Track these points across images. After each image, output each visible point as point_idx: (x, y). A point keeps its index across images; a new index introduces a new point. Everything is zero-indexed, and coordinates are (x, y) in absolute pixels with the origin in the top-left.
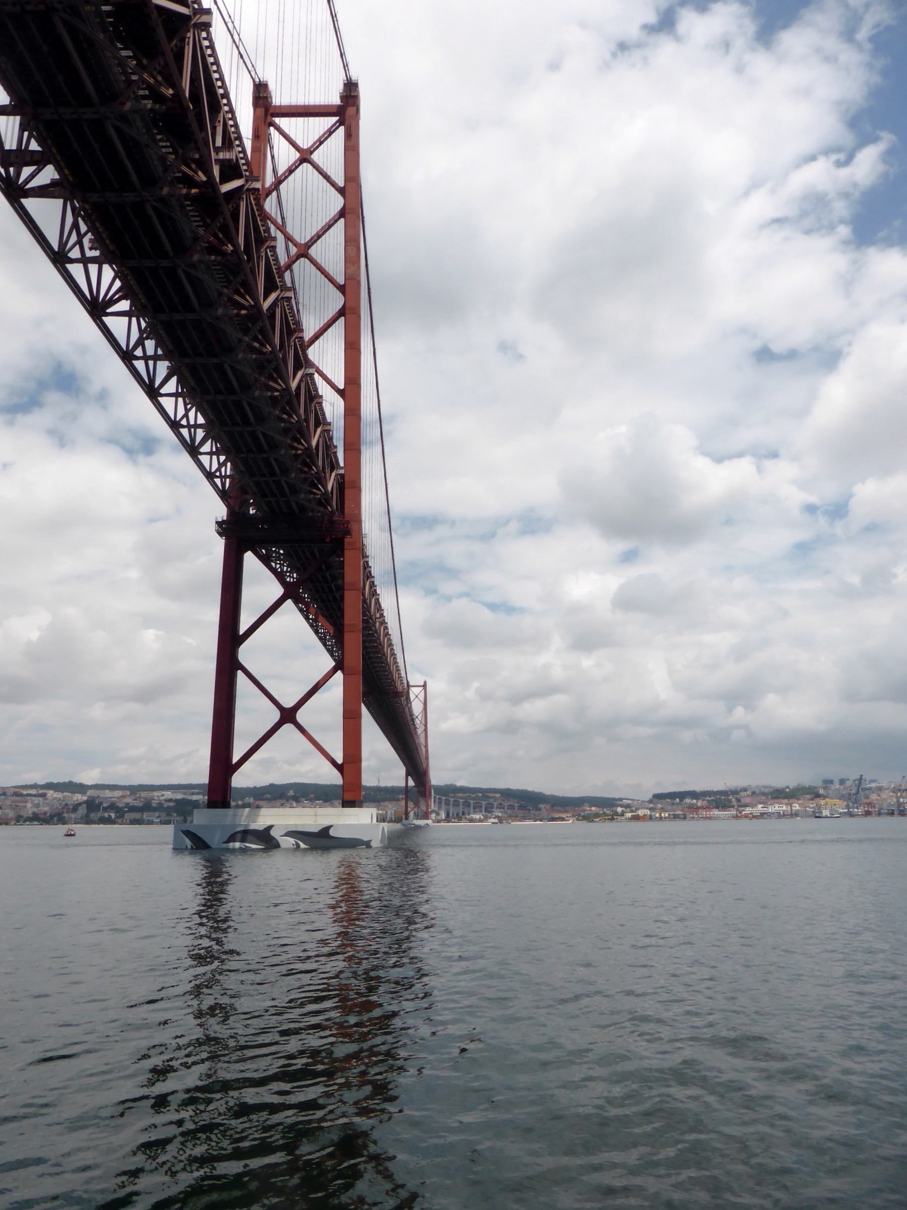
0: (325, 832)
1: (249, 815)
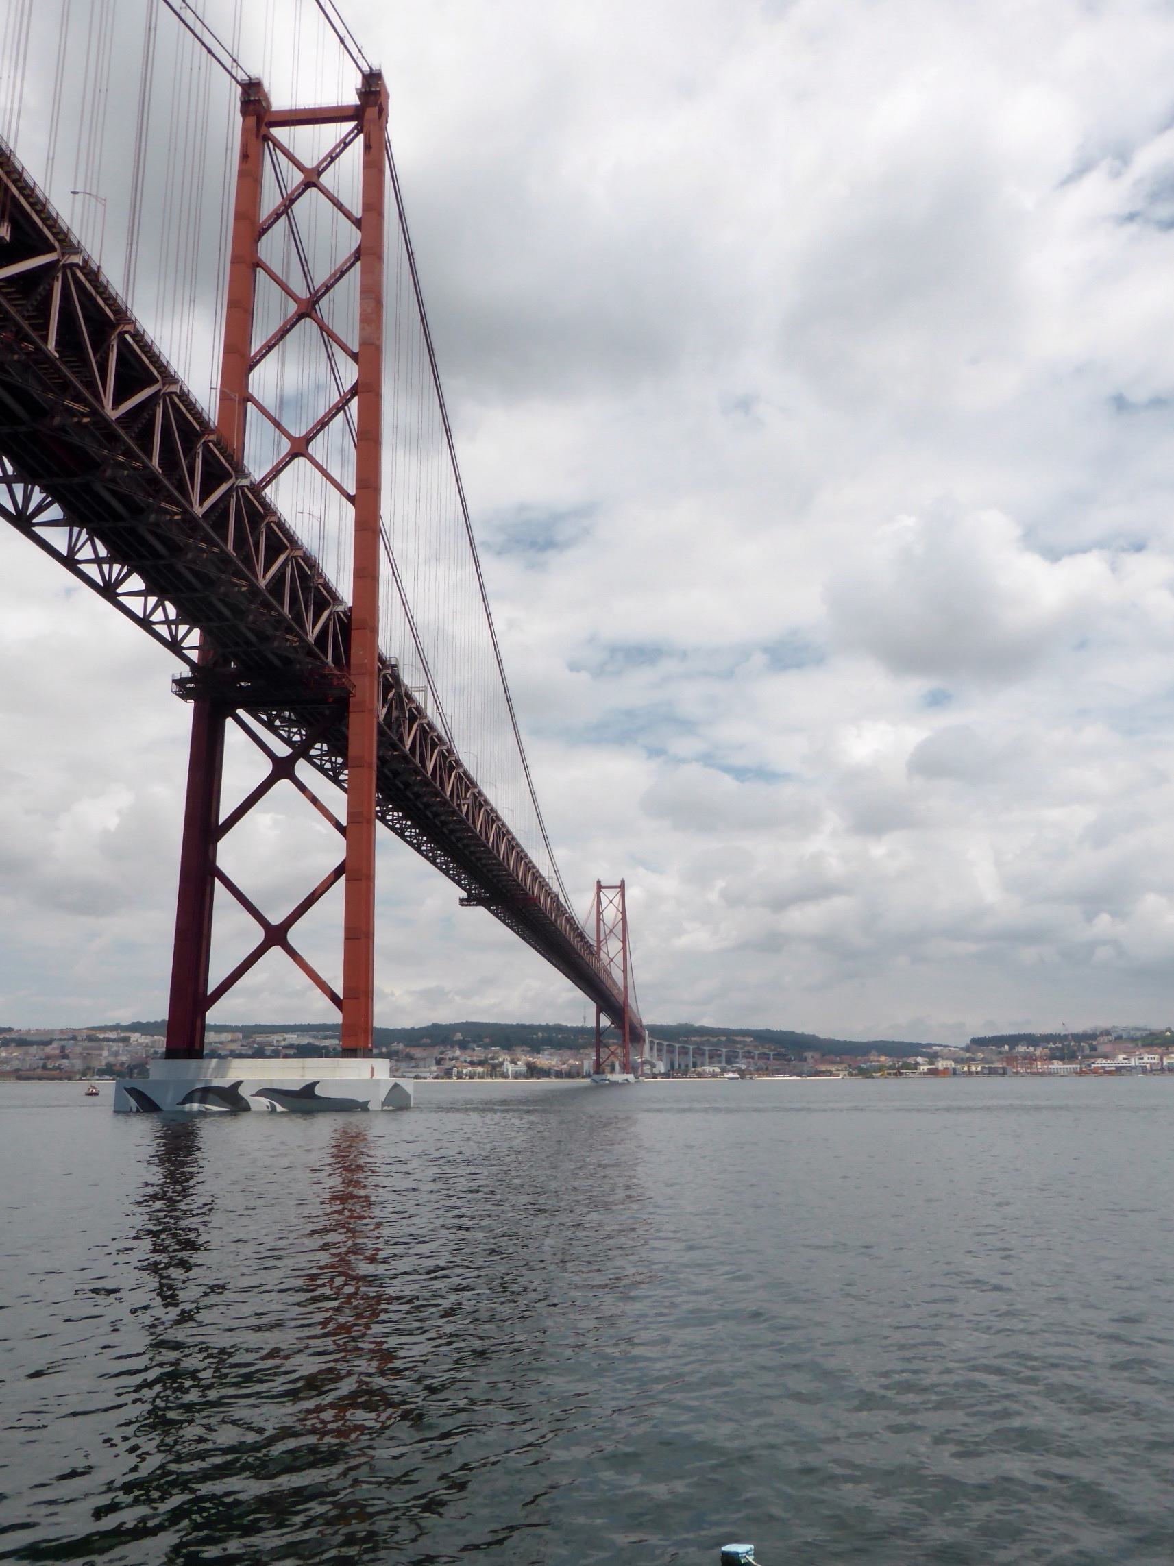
0: (308, 1091)
1: (217, 1068)
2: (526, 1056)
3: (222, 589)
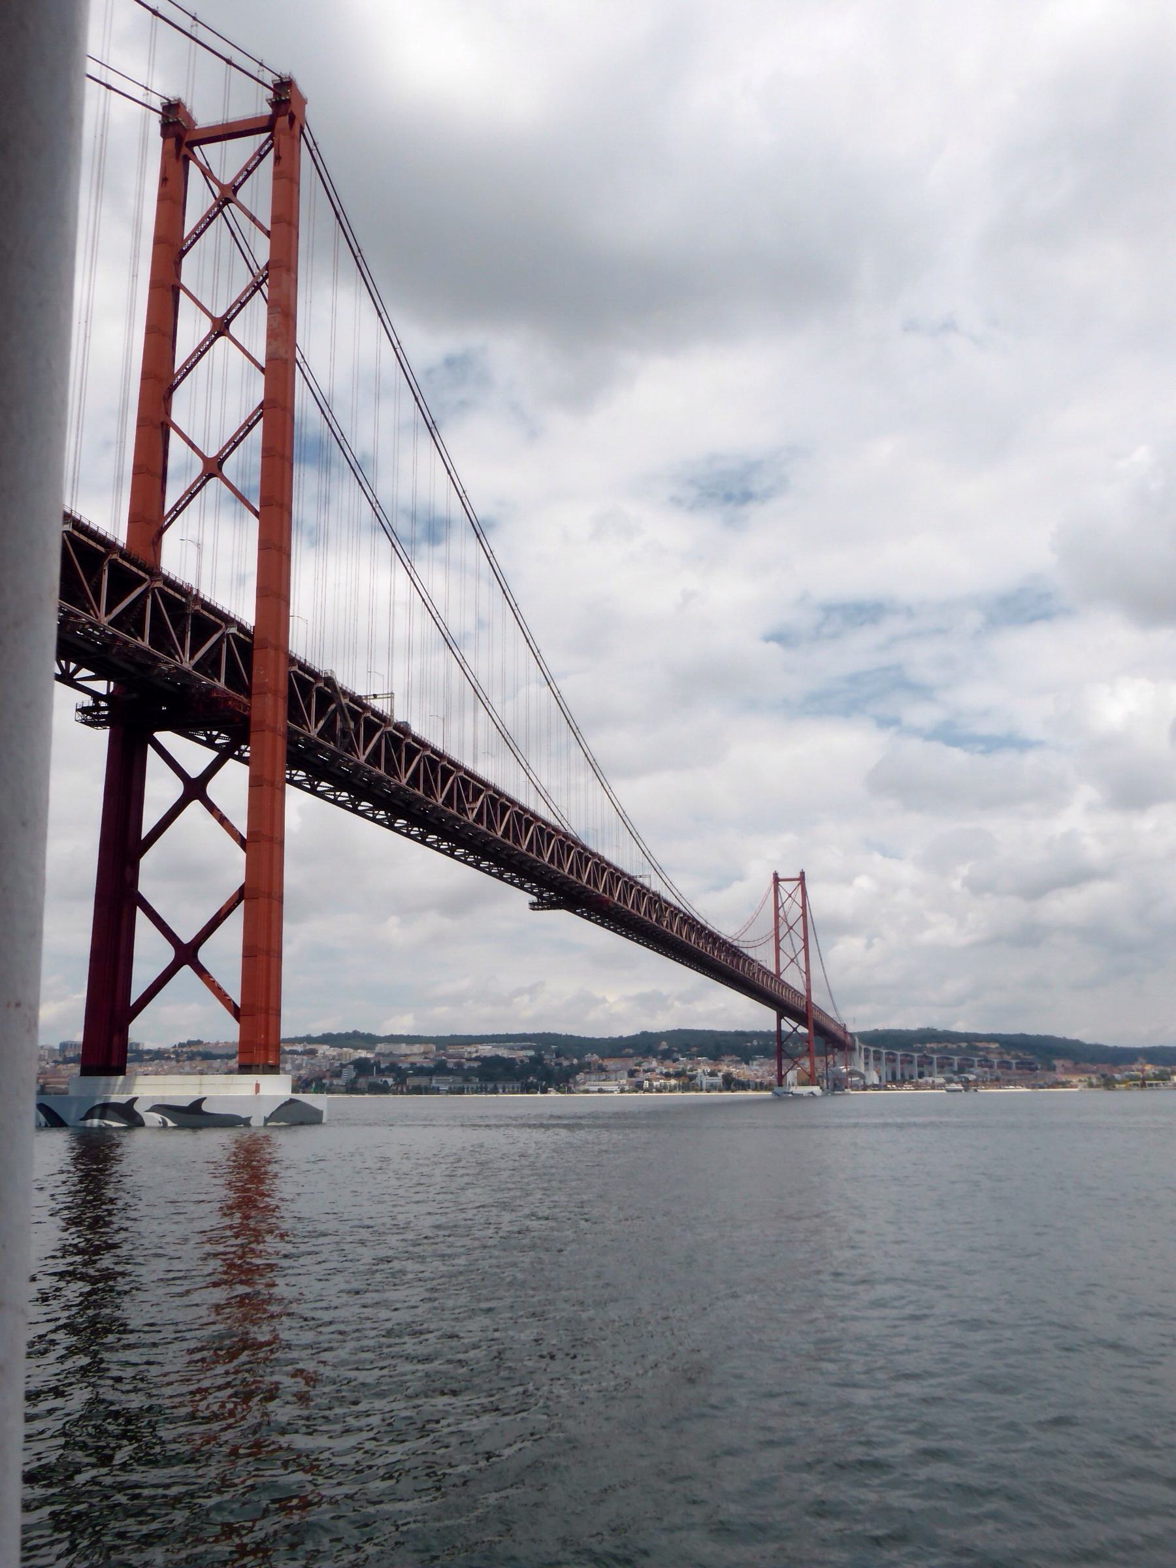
2: (728, 1066)
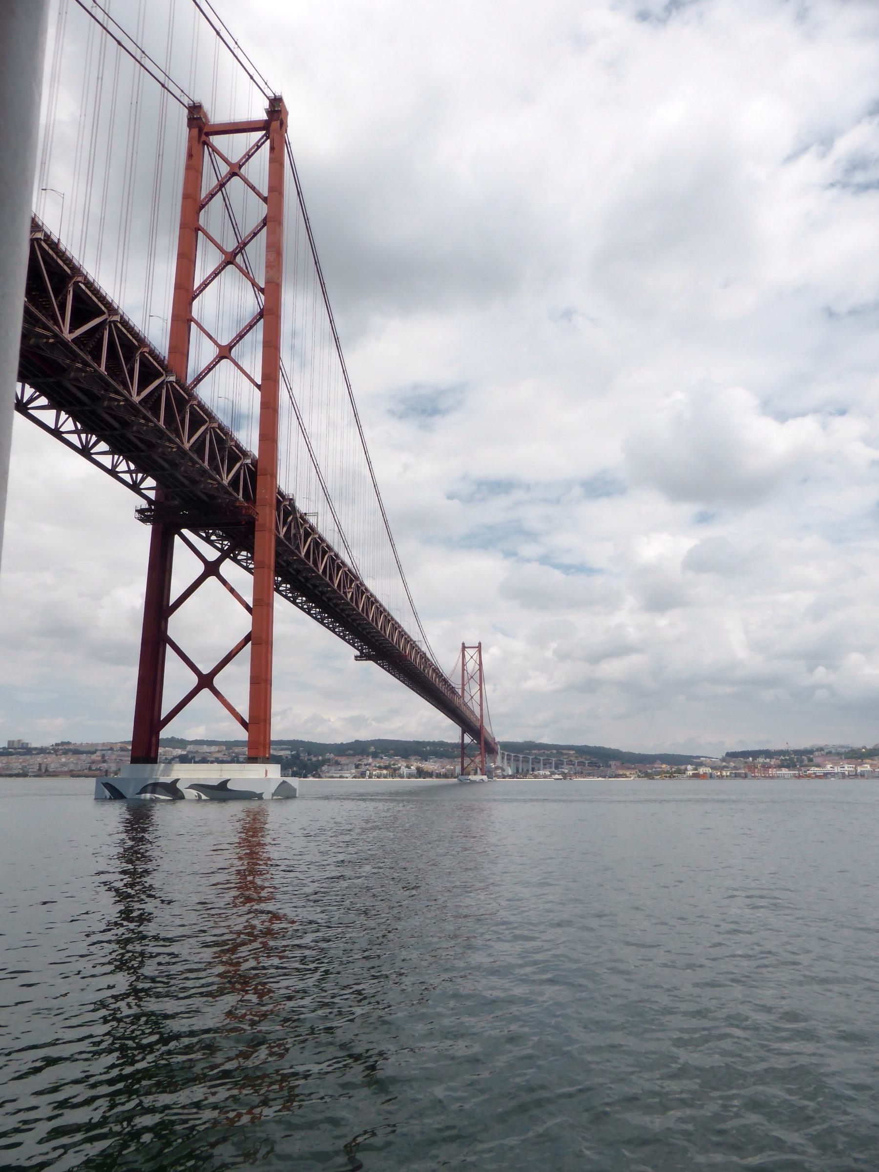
0: (223, 785)
3: (160, 450)
